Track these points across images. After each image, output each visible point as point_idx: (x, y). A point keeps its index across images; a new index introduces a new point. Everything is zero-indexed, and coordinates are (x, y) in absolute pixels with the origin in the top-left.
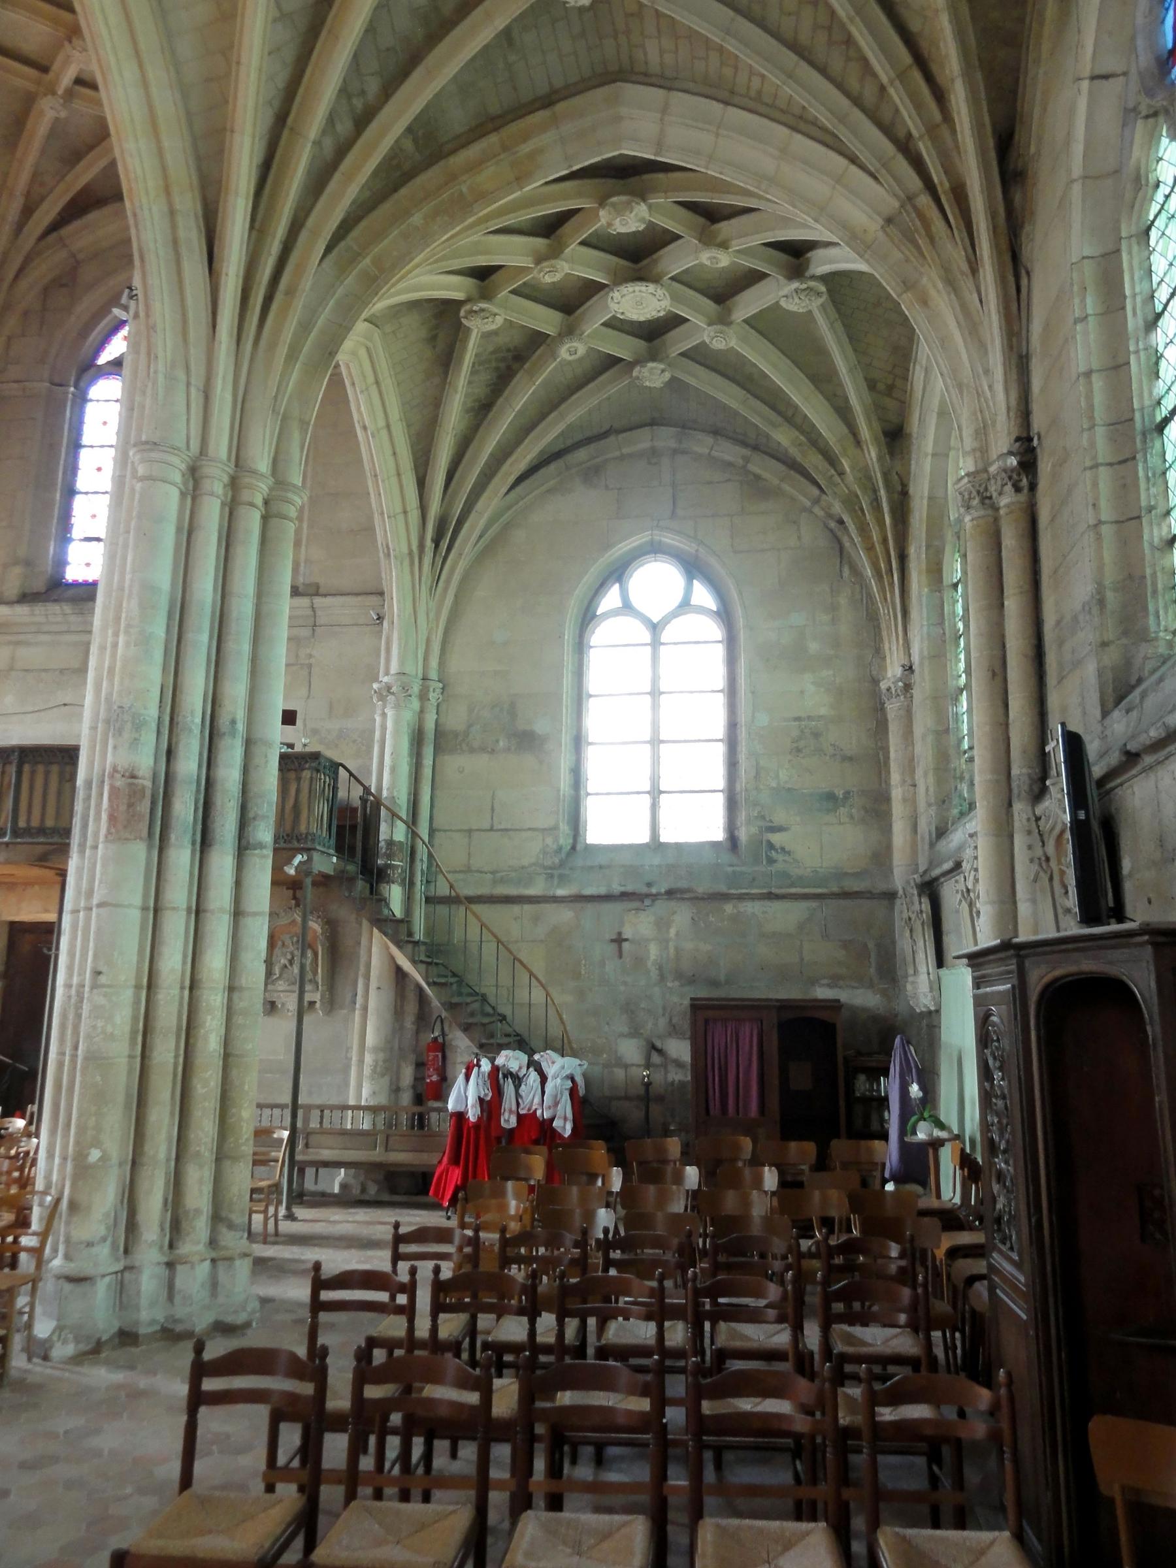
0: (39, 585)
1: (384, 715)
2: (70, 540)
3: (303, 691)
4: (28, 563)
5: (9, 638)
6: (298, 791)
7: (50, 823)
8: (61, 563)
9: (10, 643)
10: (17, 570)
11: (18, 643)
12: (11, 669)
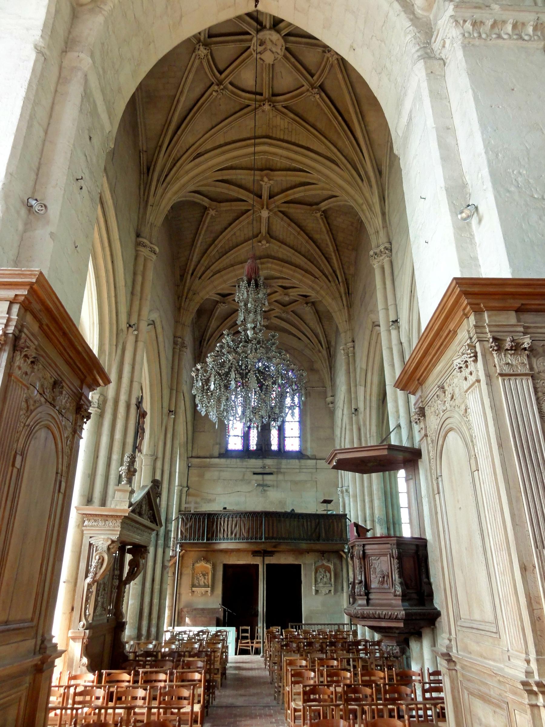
0: (223, 451)
1: (343, 498)
2: (229, 436)
3: (315, 489)
4: (220, 444)
5: (219, 469)
6: (341, 526)
7: (275, 535)
8: (227, 443)
9: (218, 471)
10: (218, 446)
11: (221, 471)
12: (219, 479)
